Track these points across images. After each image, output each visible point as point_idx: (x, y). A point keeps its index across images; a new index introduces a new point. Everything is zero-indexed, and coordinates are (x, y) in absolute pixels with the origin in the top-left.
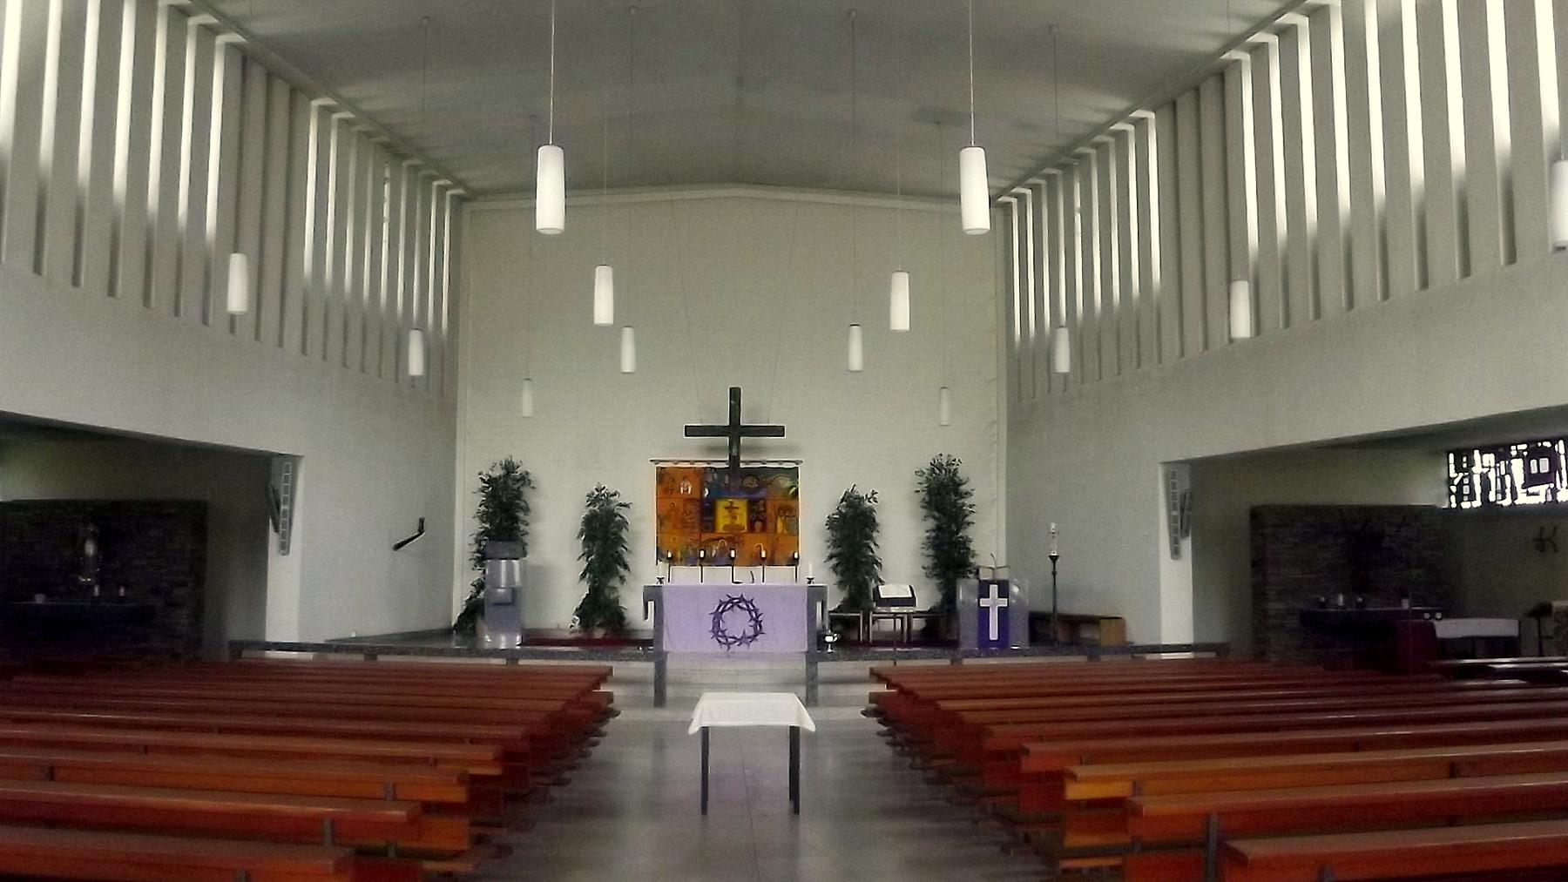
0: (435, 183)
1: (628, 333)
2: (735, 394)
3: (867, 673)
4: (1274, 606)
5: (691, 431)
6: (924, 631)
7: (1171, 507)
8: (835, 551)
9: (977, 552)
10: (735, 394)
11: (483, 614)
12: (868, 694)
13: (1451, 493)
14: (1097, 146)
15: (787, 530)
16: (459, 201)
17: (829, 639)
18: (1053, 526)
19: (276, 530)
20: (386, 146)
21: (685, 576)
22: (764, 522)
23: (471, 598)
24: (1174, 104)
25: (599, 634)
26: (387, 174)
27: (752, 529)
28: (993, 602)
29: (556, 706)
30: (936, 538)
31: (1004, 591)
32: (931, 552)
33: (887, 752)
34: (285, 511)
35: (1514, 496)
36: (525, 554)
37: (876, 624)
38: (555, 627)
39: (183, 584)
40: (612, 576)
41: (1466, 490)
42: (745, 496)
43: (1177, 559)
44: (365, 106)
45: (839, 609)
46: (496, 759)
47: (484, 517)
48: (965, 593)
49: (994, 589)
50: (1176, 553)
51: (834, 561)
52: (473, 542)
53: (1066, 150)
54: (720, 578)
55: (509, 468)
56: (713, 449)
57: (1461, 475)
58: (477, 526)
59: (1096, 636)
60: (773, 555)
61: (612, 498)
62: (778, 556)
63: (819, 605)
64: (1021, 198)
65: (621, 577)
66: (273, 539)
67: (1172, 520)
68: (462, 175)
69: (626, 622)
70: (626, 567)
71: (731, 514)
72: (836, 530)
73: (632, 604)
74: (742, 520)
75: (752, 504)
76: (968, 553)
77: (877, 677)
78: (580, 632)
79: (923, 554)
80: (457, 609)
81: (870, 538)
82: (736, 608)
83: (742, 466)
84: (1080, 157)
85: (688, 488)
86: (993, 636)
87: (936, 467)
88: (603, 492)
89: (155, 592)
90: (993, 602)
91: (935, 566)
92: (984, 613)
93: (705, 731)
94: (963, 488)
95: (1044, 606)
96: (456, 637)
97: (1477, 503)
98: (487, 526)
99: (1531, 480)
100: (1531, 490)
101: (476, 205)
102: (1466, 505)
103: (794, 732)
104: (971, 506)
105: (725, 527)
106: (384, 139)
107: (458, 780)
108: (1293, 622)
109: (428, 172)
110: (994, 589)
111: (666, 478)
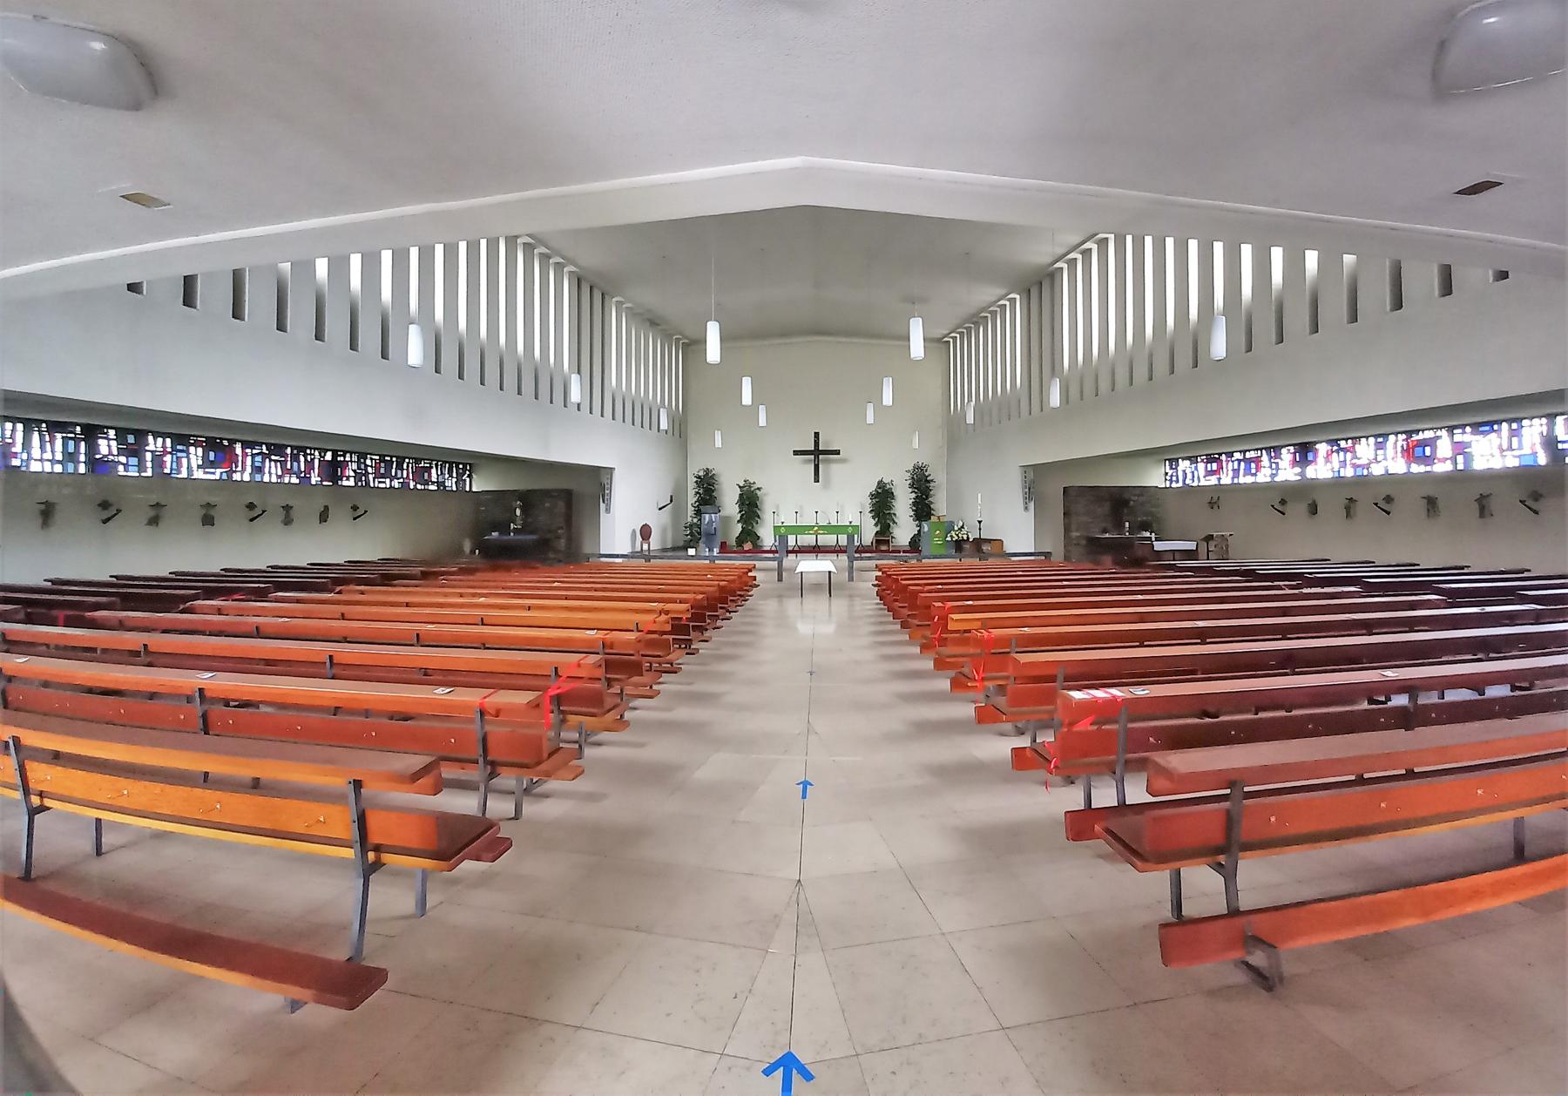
2: (817, 435)
4: (1075, 534)
10: (817, 435)
13: (1166, 479)
14: (990, 312)
19: (604, 502)
35: (1199, 481)
39: (562, 528)
41: (1174, 478)
53: (976, 315)
66: (603, 506)
89: (550, 532)
97: (1180, 484)
99: (1212, 473)
100: (1207, 478)
102: (1174, 485)
108: (1084, 542)
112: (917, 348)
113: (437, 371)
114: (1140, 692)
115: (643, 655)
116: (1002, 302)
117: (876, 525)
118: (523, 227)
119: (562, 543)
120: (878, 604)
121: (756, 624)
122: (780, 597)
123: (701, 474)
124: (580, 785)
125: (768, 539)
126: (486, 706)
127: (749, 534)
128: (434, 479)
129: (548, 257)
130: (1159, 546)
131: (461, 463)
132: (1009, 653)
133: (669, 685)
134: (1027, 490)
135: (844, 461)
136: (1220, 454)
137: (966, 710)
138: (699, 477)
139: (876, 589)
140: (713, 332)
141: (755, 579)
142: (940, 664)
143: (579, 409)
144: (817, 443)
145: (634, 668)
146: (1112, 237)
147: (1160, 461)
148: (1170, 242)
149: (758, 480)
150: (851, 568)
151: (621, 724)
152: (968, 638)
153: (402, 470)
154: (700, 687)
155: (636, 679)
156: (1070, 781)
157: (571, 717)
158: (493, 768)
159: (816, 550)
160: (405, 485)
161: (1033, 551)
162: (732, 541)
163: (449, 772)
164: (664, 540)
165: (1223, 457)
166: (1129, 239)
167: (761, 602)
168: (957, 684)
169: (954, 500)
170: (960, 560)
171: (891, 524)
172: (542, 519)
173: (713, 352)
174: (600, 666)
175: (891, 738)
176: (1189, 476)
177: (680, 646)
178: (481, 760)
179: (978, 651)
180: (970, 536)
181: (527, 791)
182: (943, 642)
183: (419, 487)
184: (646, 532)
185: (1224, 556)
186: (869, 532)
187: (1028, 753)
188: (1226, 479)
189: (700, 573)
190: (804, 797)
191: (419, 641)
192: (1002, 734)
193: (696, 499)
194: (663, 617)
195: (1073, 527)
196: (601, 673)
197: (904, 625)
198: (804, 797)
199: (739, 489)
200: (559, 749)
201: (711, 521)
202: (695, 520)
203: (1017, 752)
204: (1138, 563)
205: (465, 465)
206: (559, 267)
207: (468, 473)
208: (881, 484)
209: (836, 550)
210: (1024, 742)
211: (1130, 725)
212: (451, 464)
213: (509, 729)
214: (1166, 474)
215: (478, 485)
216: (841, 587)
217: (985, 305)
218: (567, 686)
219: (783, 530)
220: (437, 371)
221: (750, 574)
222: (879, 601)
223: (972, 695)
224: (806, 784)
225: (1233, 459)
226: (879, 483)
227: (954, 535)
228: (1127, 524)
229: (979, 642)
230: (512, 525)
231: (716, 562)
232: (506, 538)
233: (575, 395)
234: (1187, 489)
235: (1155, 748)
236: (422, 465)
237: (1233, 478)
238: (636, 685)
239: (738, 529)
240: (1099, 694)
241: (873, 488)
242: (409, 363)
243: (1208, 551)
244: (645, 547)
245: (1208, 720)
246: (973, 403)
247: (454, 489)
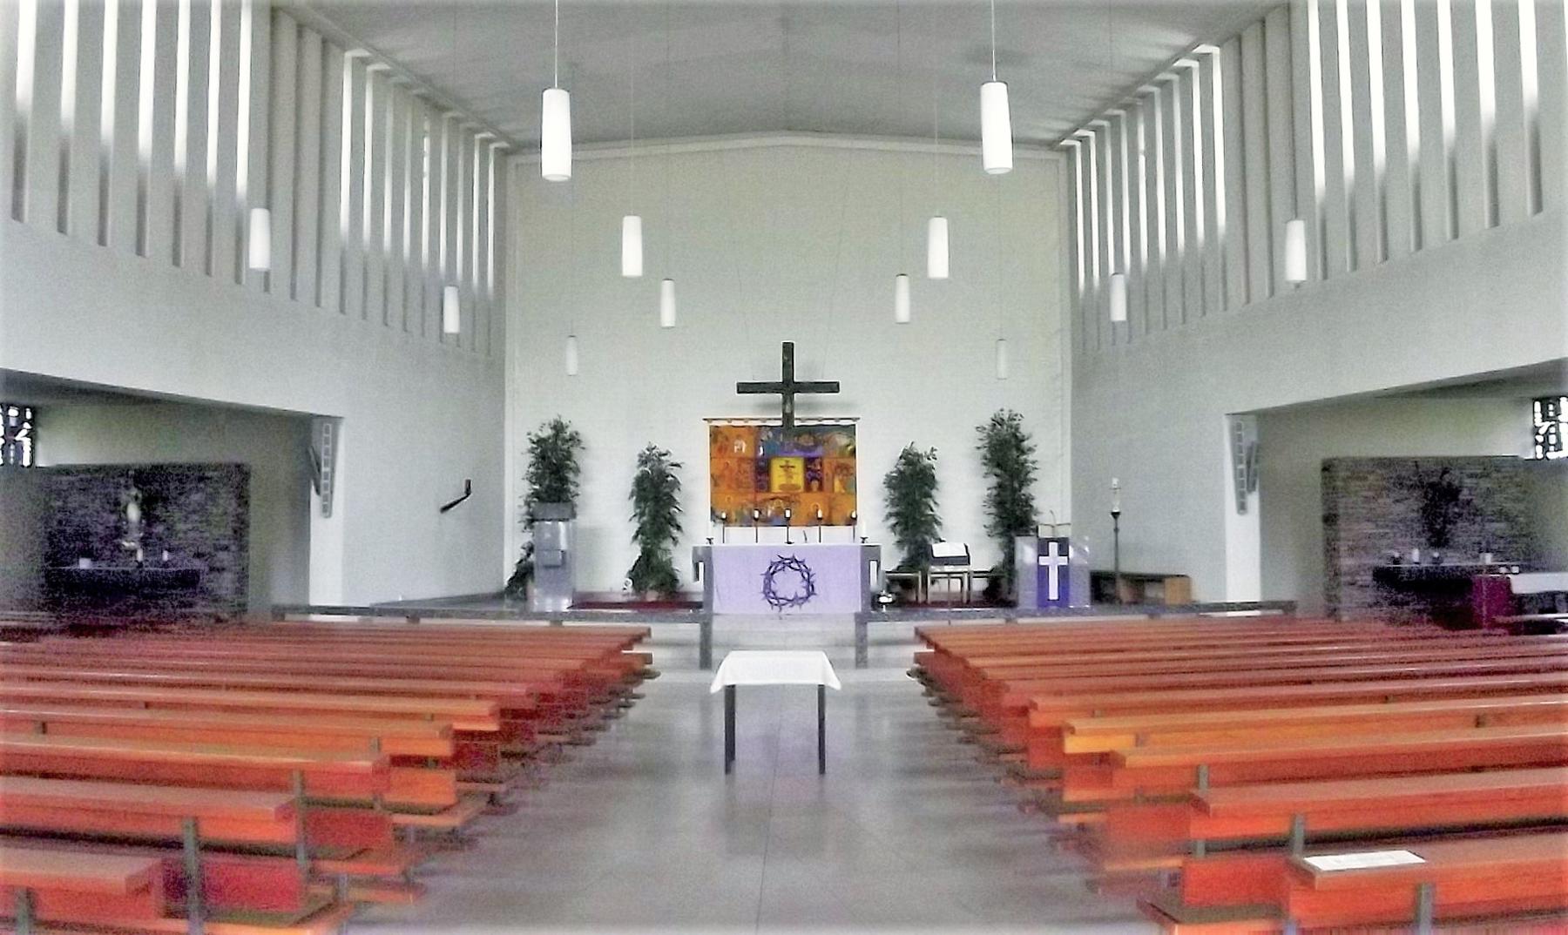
0: (478, 137)
2: (788, 349)
3: (912, 634)
4: (1346, 562)
5: (743, 388)
6: (985, 592)
7: (1237, 460)
8: (895, 510)
9: (1040, 510)
10: (788, 349)
11: (533, 578)
12: (912, 655)
13: (1536, 443)
15: (845, 489)
16: (503, 154)
17: (883, 600)
18: (1115, 481)
19: (318, 491)
20: (425, 99)
21: (740, 536)
22: (821, 481)
23: (521, 561)
24: (1239, 39)
25: (652, 596)
26: (427, 126)
27: (808, 488)
28: (1053, 560)
29: (575, 664)
30: (998, 495)
31: (1063, 552)
32: (993, 510)
33: (931, 713)
34: (326, 474)
36: (574, 515)
37: (936, 585)
38: (608, 590)
39: (226, 548)
40: (664, 538)
41: (1553, 439)
42: (802, 454)
43: (1242, 514)
44: (400, 57)
45: (899, 569)
46: (491, 715)
47: (536, 478)
48: (1026, 552)
49: (1053, 547)
50: (1242, 507)
51: (893, 521)
52: (522, 503)
54: (773, 538)
55: (558, 428)
56: (767, 407)
57: (1548, 424)
58: (526, 488)
59: (1161, 595)
60: (830, 516)
61: (663, 458)
62: (836, 516)
63: (873, 565)
65: (674, 539)
66: (315, 500)
67: (1238, 474)
68: (504, 127)
69: (680, 584)
70: (679, 528)
71: (787, 473)
72: (894, 489)
73: (683, 565)
74: (798, 479)
75: (809, 461)
76: (1031, 511)
77: (922, 637)
78: (632, 595)
79: (985, 513)
80: (509, 571)
81: (930, 496)
82: (787, 568)
83: (797, 423)
84: (1144, 96)
85: (742, 446)
86: (1053, 595)
87: (997, 422)
88: (654, 451)
89: (198, 555)
90: (1053, 560)
91: (995, 526)
92: (1043, 572)
93: (730, 691)
94: (1026, 444)
95: (1106, 565)
96: (508, 601)
98: (537, 487)
101: (520, 159)
102: (1552, 455)
103: (821, 689)
104: (1033, 462)
105: (782, 487)
106: (423, 91)
107: (441, 733)
108: (1368, 578)
109: (469, 125)
110: (1053, 547)
111: (720, 438)
130: (1524, 584)
134: (1243, 466)
141: (647, 659)
143: (267, 288)
144: (788, 365)
147: (1521, 402)
161: (1257, 599)
172: (183, 524)
205: (22, 410)
207: (27, 425)
221: (637, 650)
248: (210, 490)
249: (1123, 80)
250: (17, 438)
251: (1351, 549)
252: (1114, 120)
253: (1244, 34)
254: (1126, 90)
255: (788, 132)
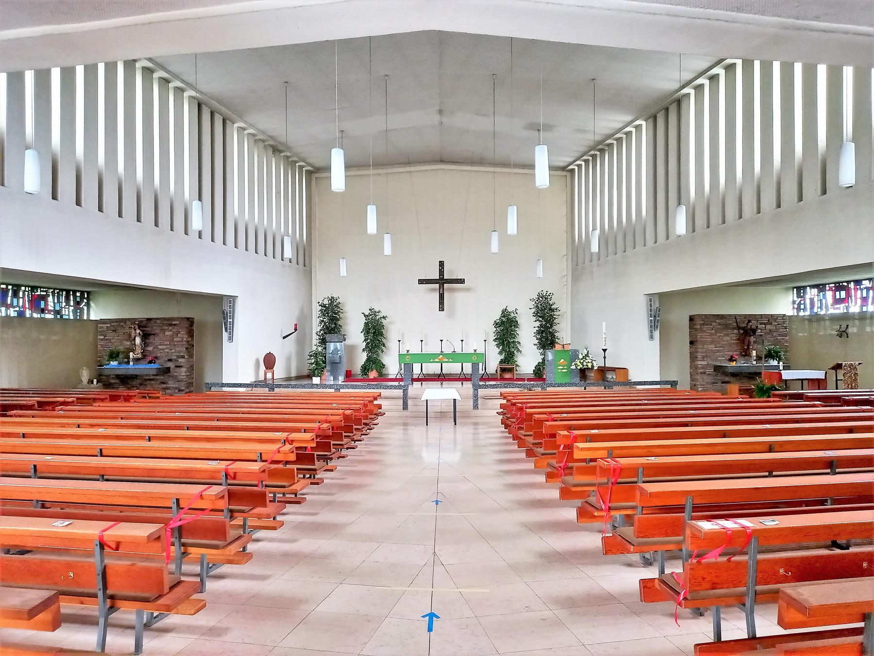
1: (387, 238)
2: (441, 264)
10: (441, 264)
16: (309, 173)
39: (183, 357)
41: (802, 307)
44: (261, 127)
57: (800, 299)
64: (579, 166)
66: (225, 335)
68: (309, 161)
89: (170, 360)
97: (808, 313)
100: (836, 306)
101: (317, 175)
102: (802, 313)
106: (271, 143)
108: (710, 371)
112: (542, 177)
113: (54, 197)
114: (771, 522)
115: (266, 486)
116: (628, 129)
117: (500, 353)
118: (142, 53)
119: (183, 373)
120: (502, 432)
121: (381, 453)
122: (405, 424)
123: (326, 302)
124: (202, 619)
125: (392, 367)
126: (105, 539)
127: (374, 363)
128: (50, 308)
129: (167, 81)
130: (786, 375)
131: (79, 291)
132: (636, 482)
133: (292, 515)
134: (652, 319)
135: (468, 290)
136: (848, 282)
137: (592, 540)
138: (325, 306)
139: (501, 417)
140: (337, 160)
141: (380, 407)
142: (566, 493)
143: (200, 237)
144: (441, 272)
145: (259, 499)
146: (739, 63)
147: (788, 289)
148: (798, 68)
149: (384, 308)
150: (476, 397)
151: (244, 556)
152: (595, 467)
153: (18, 298)
154: (326, 517)
155: (259, 510)
156: (699, 613)
157: (191, 550)
158: (113, 602)
159: (441, 378)
160: (21, 314)
162: (357, 369)
163: (67, 607)
164: (288, 369)
165: (852, 285)
166: (757, 64)
167: (386, 430)
168: (583, 513)
169: (579, 328)
170: (585, 389)
171: (515, 352)
173: (338, 179)
174: (223, 497)
175: (517, 569)
176: (817, 304)
177: (304, 477)
178: (100, 594)
179: (605, 480)
180: (595, 365)
181: (147, 626)
182: (568, 470)
183: (35, 315)
184: (269, 361)
185: (853, 383)
186: (493, 361)
187: (657, 584)
188: (855, 308)
189: (324, 401)
190: (430, 629)
191: (36, 472)
192: (630, 565)
193: (319, 328)
194: (288, 447)
195: (699, 356)
196: (223, 504)
197: (530, 453)
198: (430, 629)
199: (364, 318)
200: (179, 583)
201: (336, 349)
202: (320, 349)
203: (646, 584)
204: (765, 392)
205: (82, 293)
206: (179, 91)
207: (85, 301)
208: (505, 313)
209: (462, 378)
210: (652, 573)
211: (760, 557)
212: (68, 292)
213: (129, 563)
214: (794, 302)
215: (96, 312)
216: (466, 416)
217: (611, 132)
218: (188, 518)
219: (408, 360)
220: (54, 197)
221: (375, 402)
222: (503, 429)
223: (598, 524)
224: (432, 616)
225: (862, 287)
226: (503, 312)
227: (579, 364)
228: (754, 353)
229: (605, 471)
230: (131, 354)
231: (341, 390)
232: (124, 366)
233: (197, 221)
234: (814, 319)
235: (785, 580)
236: (39, 293)
237: (862, 306)
238: (259, 517)
239: (363, 357)
240: (730, 524)
241: (497, 316)
242: (26, 190)
243: (837, 380)
244: (269, 376)
245: (838, 551)
246: (598, 232)
247: (72, 317)
248: (175, 330)
249: (598, 138)
250: (81, 306)
251: (703, 357)
252: (594, 157)
253: (657, 115)
254: (601, 142)
255: (441, 163)
